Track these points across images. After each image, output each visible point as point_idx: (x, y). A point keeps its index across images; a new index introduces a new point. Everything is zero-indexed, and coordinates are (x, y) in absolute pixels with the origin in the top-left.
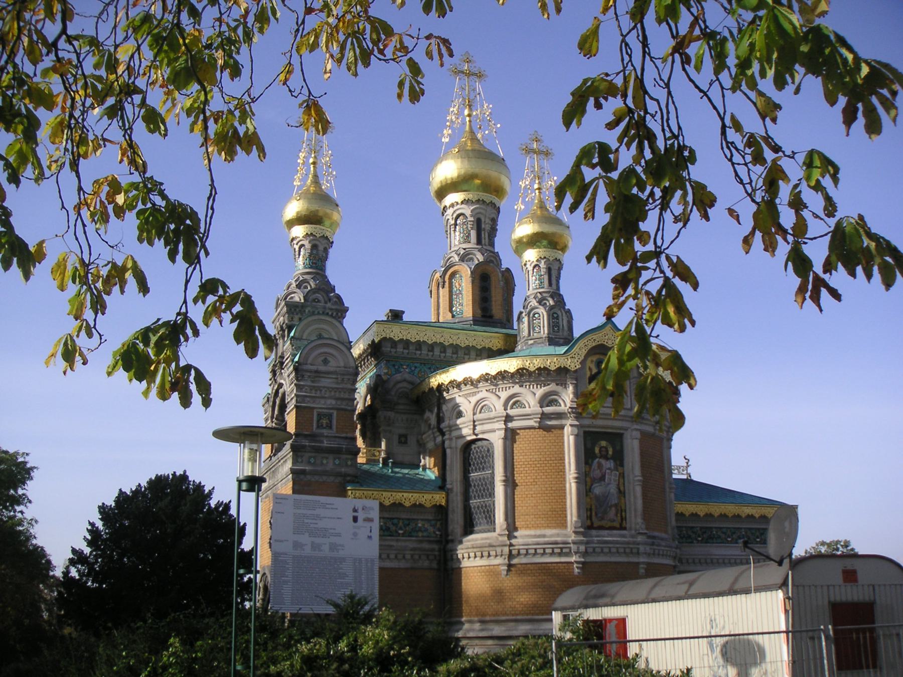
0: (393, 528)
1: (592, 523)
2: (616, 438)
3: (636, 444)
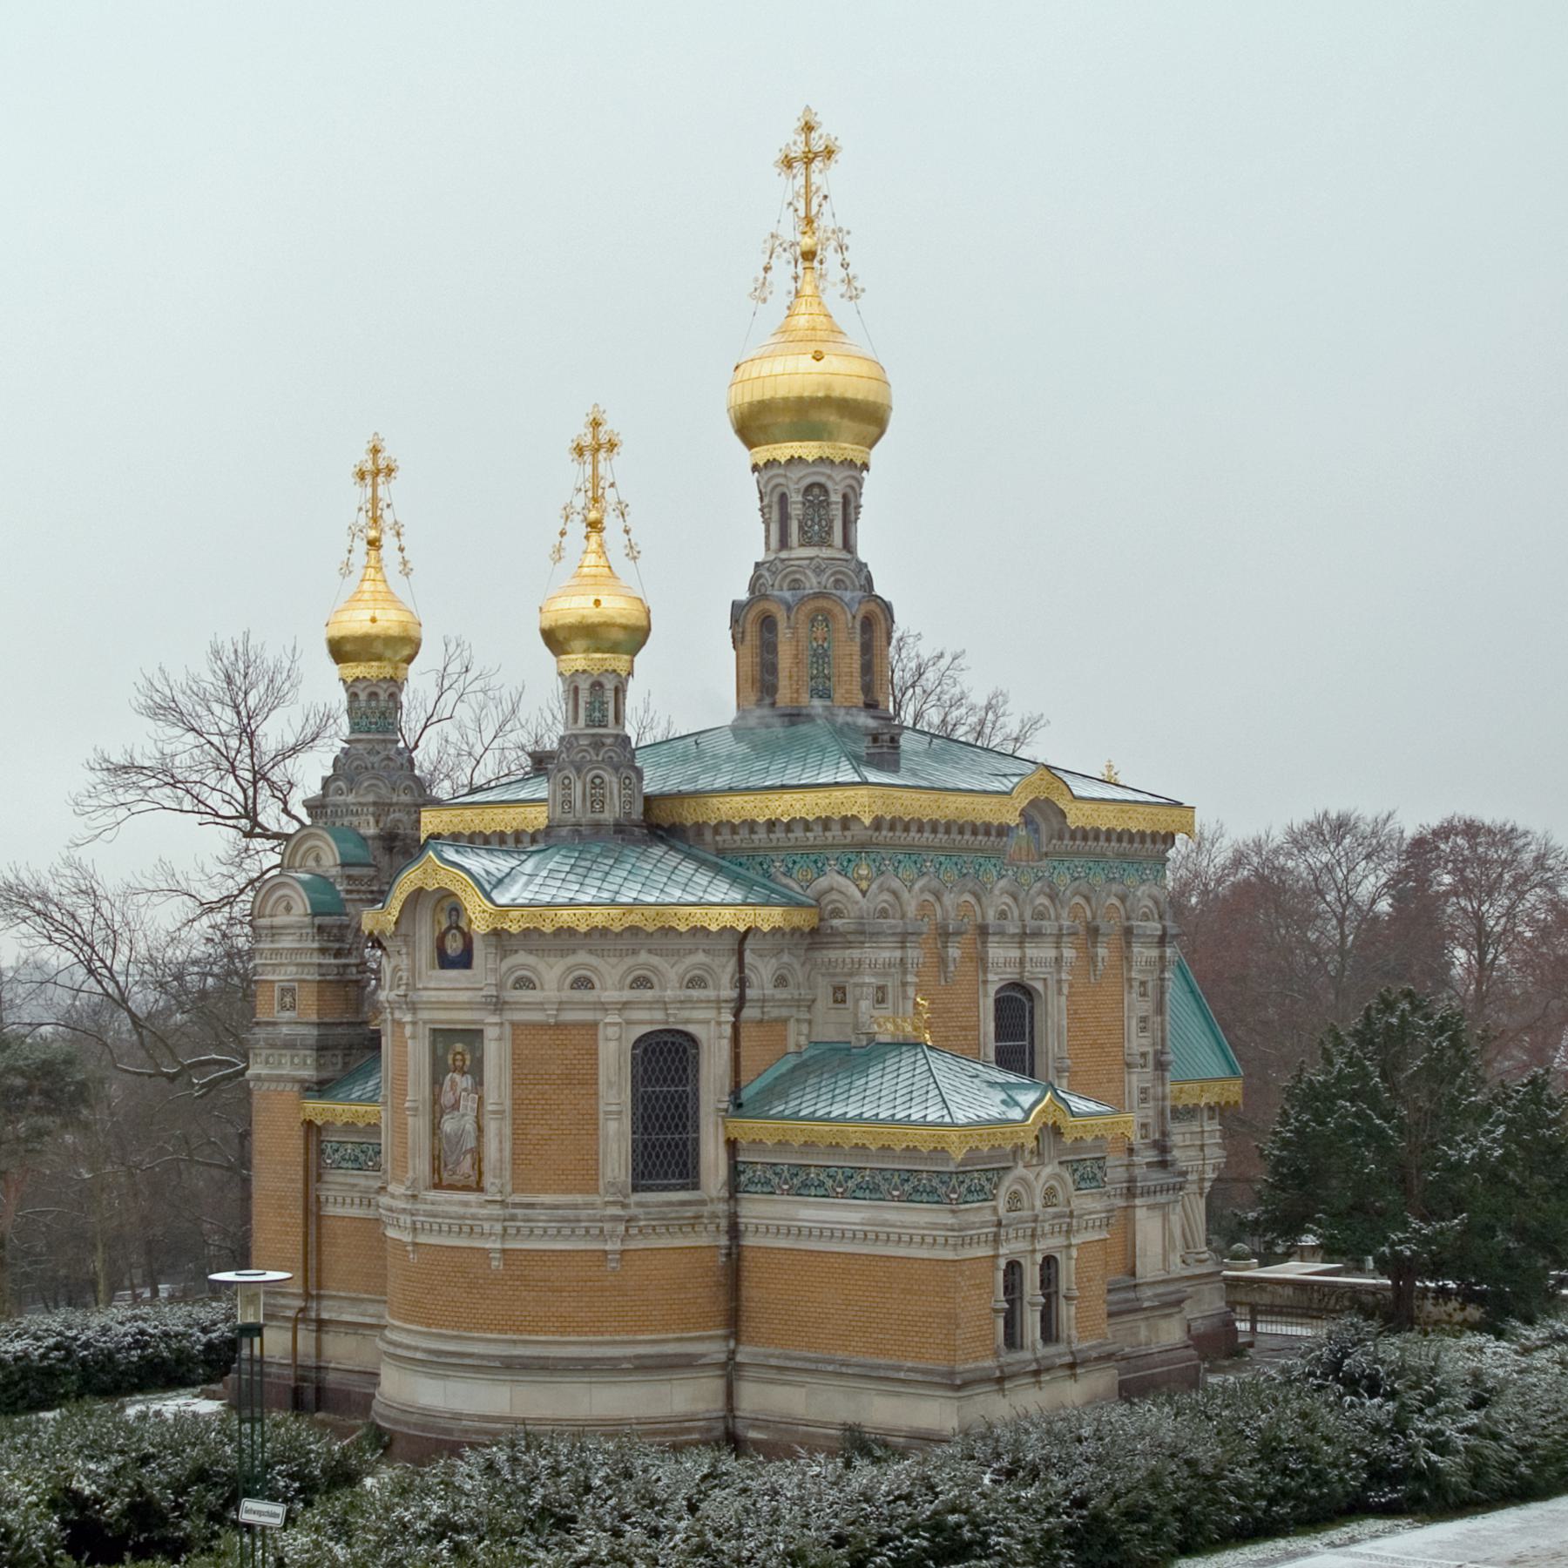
0: (362, 1158)
2: (473, 1036)
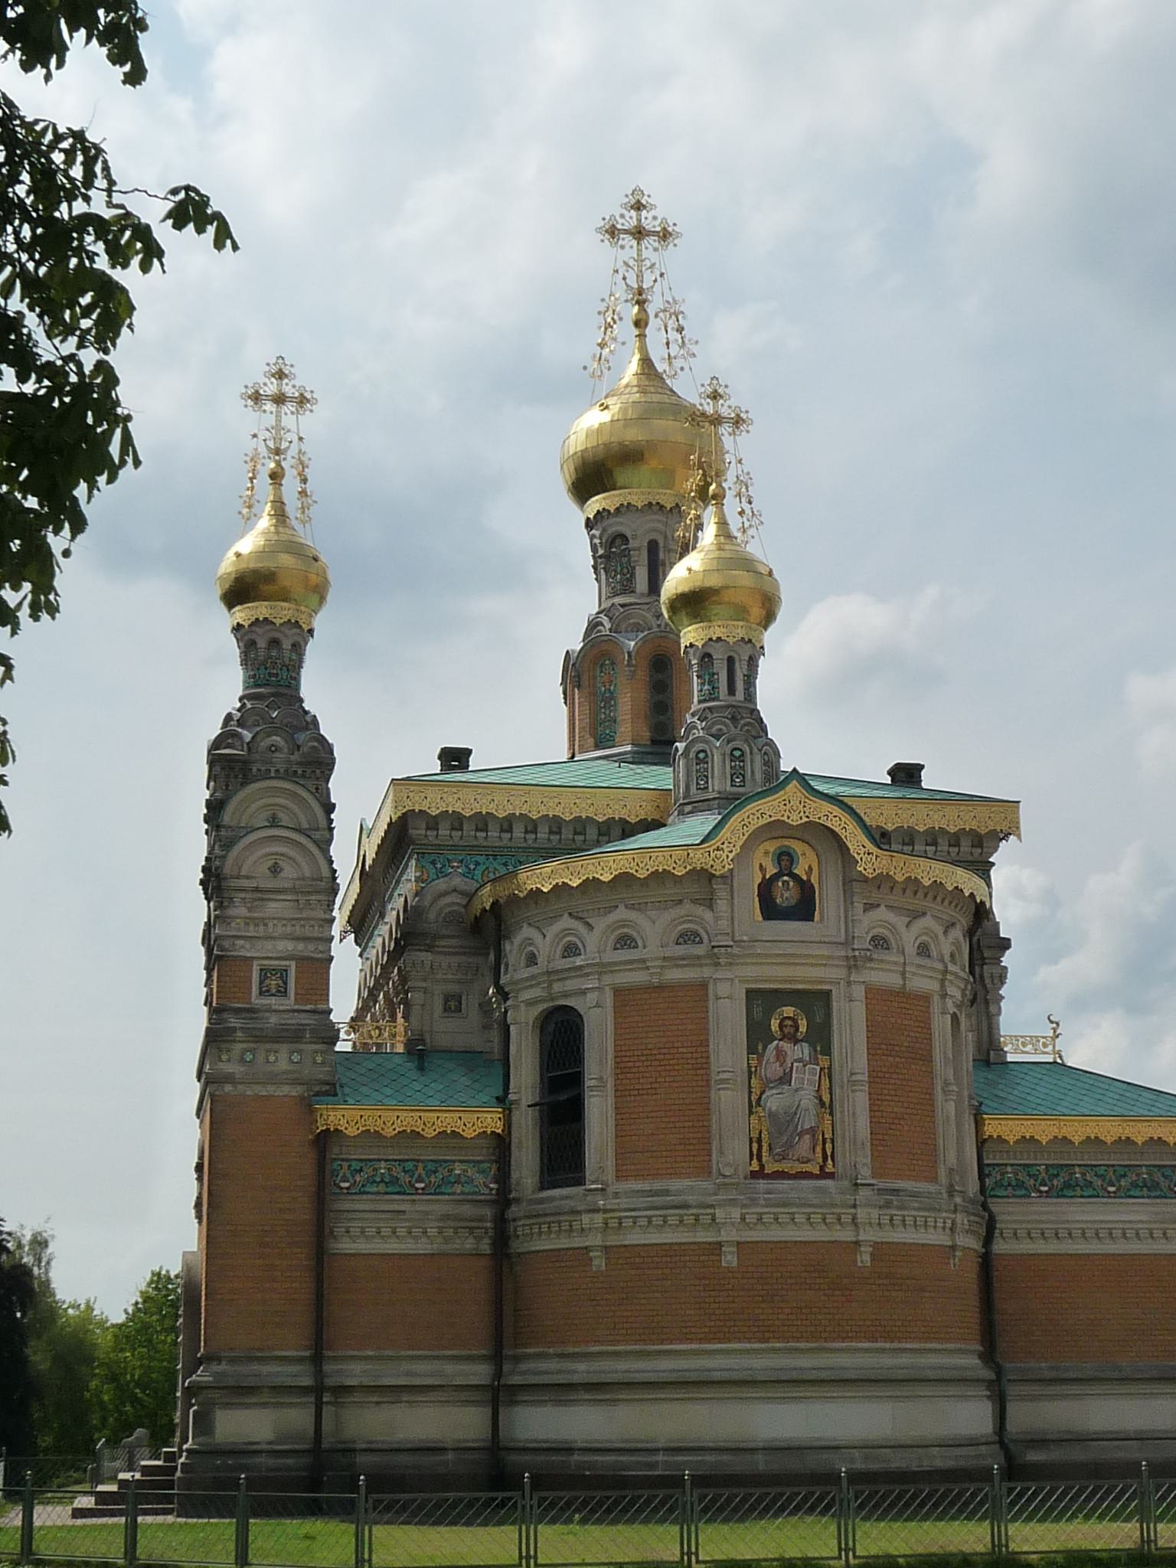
0: (404, 1178)
1: (762, 1167)
2: (816, 1002)
3: (859, 1010)
